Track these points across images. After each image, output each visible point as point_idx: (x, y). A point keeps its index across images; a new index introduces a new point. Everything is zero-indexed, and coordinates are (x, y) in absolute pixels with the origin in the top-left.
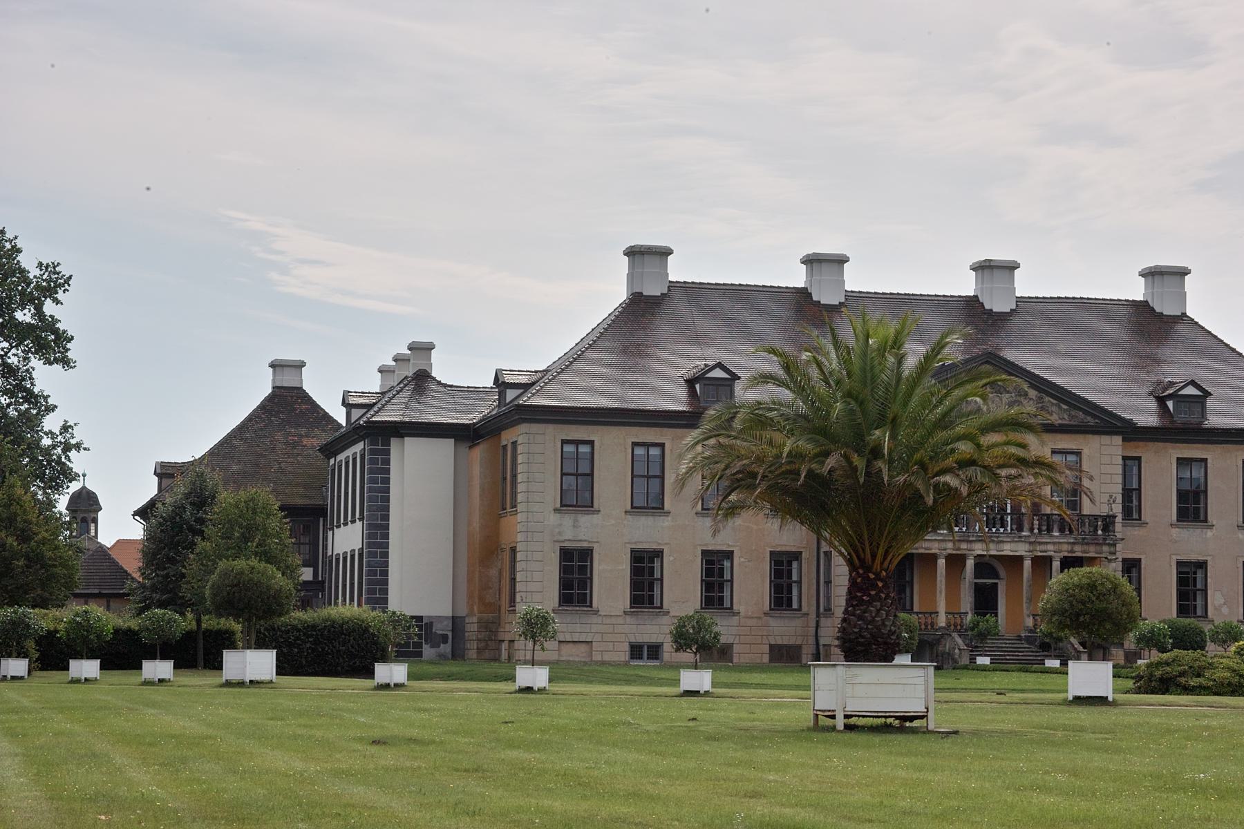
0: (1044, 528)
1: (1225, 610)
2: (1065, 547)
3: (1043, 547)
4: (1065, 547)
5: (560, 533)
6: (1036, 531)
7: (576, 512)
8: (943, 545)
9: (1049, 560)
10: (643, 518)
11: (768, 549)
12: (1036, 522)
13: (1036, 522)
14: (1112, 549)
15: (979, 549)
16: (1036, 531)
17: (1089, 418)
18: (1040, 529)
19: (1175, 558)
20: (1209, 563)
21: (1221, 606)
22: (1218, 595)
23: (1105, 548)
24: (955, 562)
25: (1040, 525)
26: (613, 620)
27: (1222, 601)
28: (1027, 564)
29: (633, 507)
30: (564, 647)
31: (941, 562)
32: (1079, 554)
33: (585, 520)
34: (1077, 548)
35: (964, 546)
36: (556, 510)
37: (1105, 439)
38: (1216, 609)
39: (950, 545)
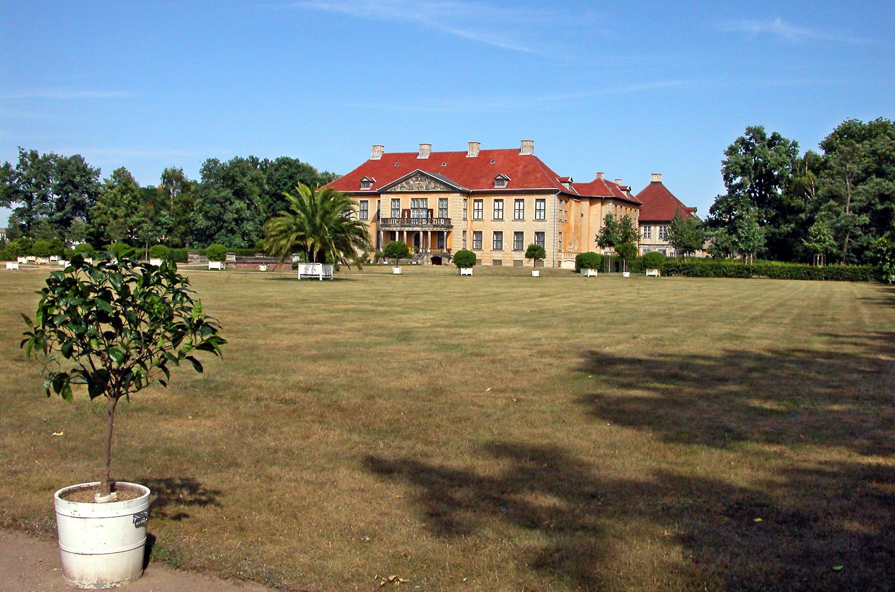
15: (407, 229)
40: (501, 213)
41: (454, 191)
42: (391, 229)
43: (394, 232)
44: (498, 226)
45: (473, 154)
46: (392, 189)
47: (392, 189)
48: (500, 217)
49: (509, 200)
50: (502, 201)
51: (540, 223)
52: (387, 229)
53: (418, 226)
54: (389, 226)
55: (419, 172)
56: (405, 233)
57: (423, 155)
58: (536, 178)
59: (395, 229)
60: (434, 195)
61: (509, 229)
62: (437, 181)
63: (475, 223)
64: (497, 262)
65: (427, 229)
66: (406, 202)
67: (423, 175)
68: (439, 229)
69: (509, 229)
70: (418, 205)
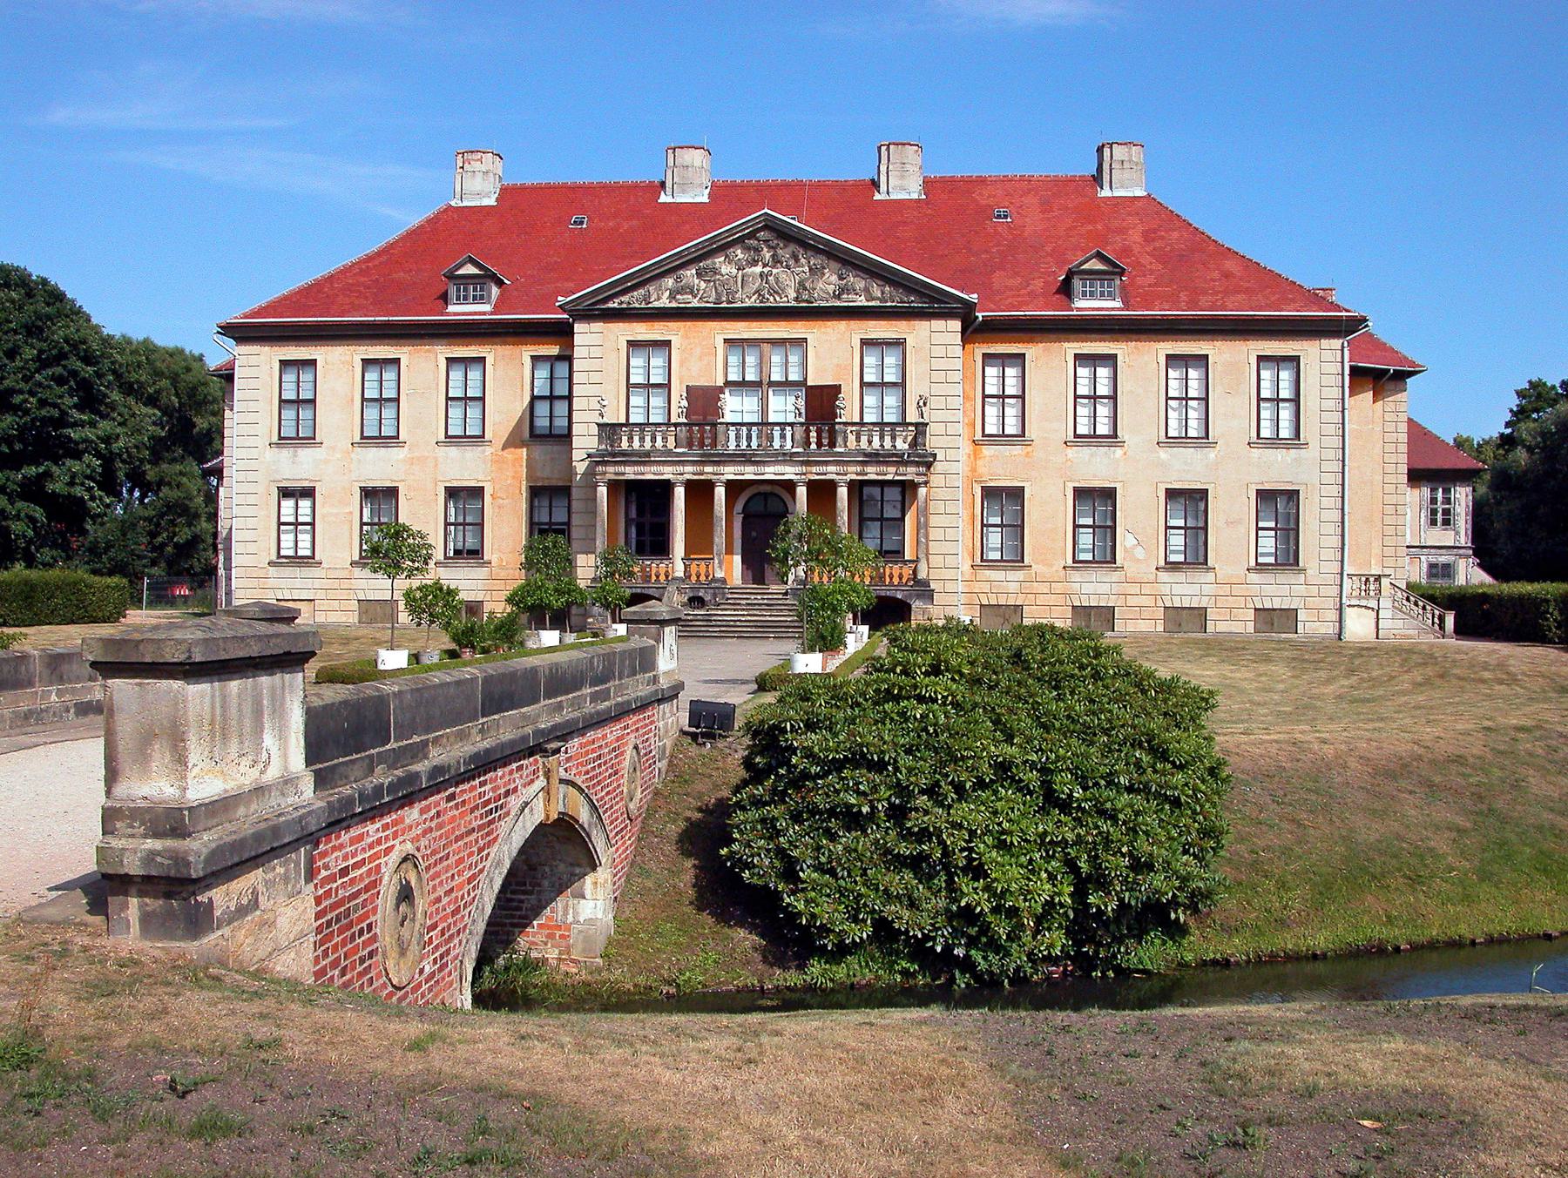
0: (825, 441)
6: (814, 446)
7: (296, 446)
8: (680, 469)
9: (831, 486)
12: (813, 434)
13: (813, 434)
15: (730, 472)
16: (814, 446)
18: (819, 444)
19: (1070, 486)
24: (700, 492)
25: (819, 438)
28: (802, 491)
29: (363, 437)
31: (680, 492)
33: (305, 454)
34: (869, 469)
35: (708, 469)
37: (938, 324)
39: (689, 469)
40: (1103, 410)
41: (932, 306)
42: (649, 473)
43: (666, 487)
44: (1095, 468)
45: (903, 184)
46: (634, 300)
47: (634, 300)
48: (1103, 429)
49: (1142, 362)
50: (1111, 360)
51: (1279, 455)
52: (630, 473)
53: (787, 458)
54: (643, 458)
55: (771, 225)
56: (720, 492)
57: (685, 186)
58: (1227, 275)
59: (667, 473)
60: (841, 326)
61: (1140, 474)
62: (848, 262)
63: (988, 451)
64: (1275, 619)
65: (831, 472)
66: (700, 354)
67: (785, 235)
68: (890, 473)
69: (1140, 474)
70: (762, 365)
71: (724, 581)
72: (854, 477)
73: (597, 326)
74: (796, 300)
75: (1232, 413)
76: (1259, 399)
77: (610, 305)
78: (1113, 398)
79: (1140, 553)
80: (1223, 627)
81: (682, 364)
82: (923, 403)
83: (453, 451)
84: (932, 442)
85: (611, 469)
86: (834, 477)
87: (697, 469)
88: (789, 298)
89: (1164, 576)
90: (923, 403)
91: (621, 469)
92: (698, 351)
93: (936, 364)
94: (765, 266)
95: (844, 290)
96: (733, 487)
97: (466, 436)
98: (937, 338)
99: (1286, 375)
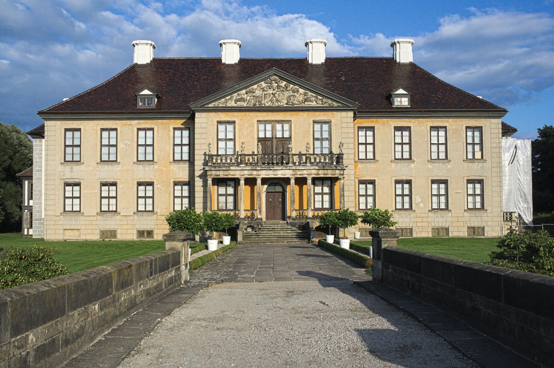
1: (421, 205)
2: (314, 172)
3: (301, 172)
4: (314, 172)
5: (64, 175)
8: (243, 173)
10: (106, 166)
11: (172, 180)
14: (342, 172)
17: (334, 103)
20: (413, 181)
21: (419, 203)
22: (418, 197)
23: (337, 172)
26: (91, 218)
27: (420, 200)
30: (66, 232)
32: (322, 176)
33: (76, 168)
35: (255, 173)
36: (61, 163)
37: (344, 114)
38: (416, 204)
39: (246, 172)
60: (305, 114)
63: (360, 166)
71: (261, 219)
72: (314, 176)
73: (204, 115)
74: (287, 104)
75: (457, 150)
76: (467, 144)
77: (210, 105)
78: (410, 144)
79: (421, 205)
80: (419, 235)
81: (240, 130)
82: (341, 145)
83: (141, 167)
84: (345, 162)
85: (213, 172)
86: (306, 176)
87: (250, 172)
88: (284, 103)
89: (431, 214)
90: (341, 145)
91: (218, 173)
92: (247, 125)
93: (344, 130)
94: (274, 90)
95: (306, 100)
96: (265, 181)
97: (145, 161)
98: (344, 120)
99: (477, 134)
